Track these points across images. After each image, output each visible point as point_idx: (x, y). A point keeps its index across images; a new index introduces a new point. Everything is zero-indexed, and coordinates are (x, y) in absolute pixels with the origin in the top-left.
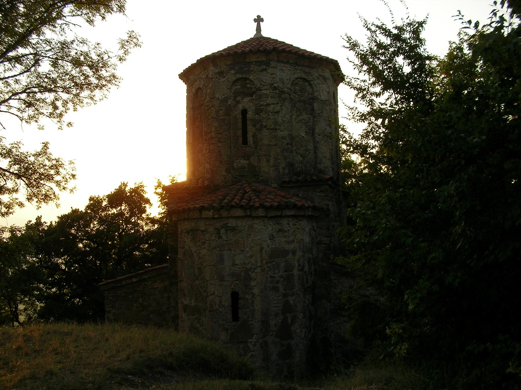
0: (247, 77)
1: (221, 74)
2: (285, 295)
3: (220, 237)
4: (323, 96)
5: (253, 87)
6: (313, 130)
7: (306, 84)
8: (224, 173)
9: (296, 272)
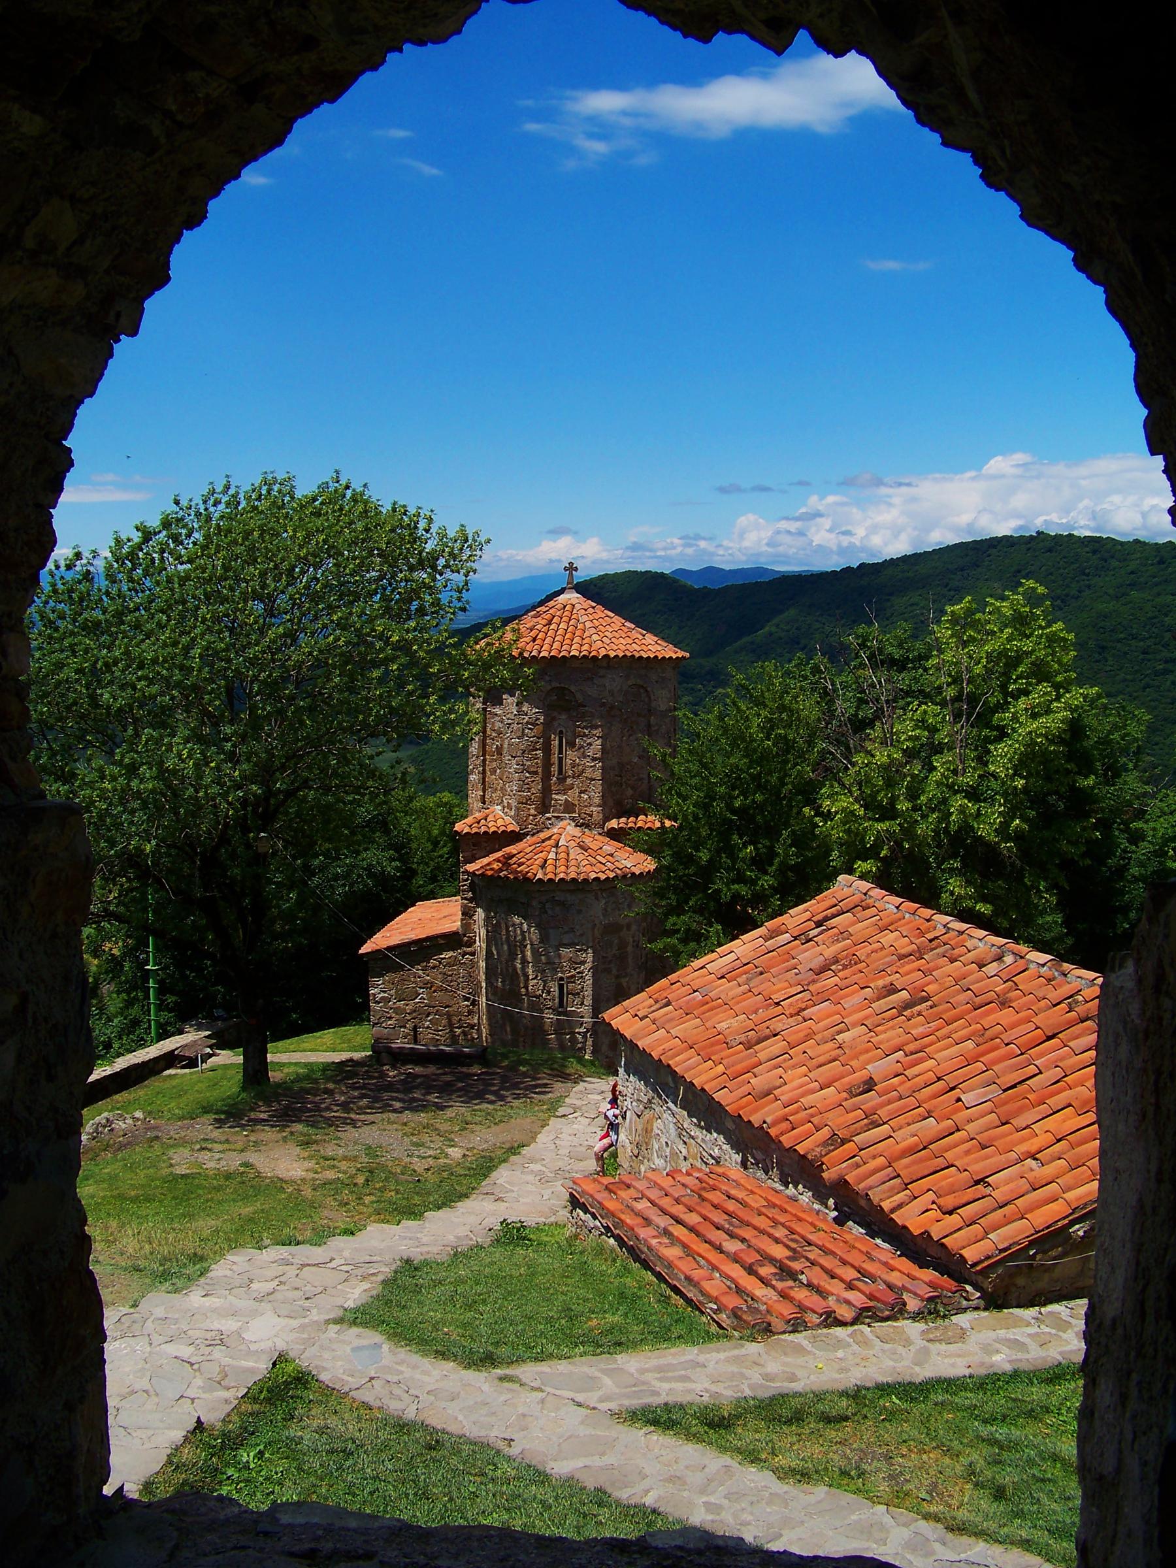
2: (617, 977)
3: (546, 912)
9: (630, 949)
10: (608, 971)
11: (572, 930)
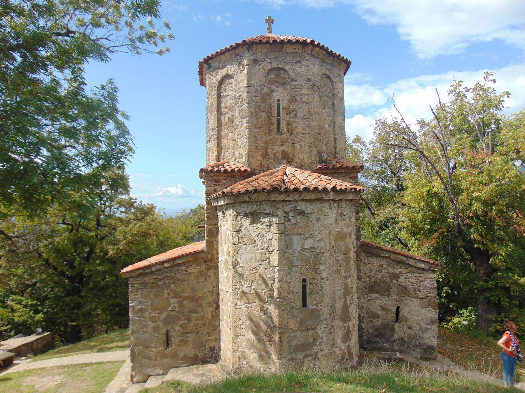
0: (282, 67)
1: (255, 62)
3: (289, 220)
4: (340, 95)
5: (287, 77)
6: (334, 123)
7: (328, 81)
8: (260, 158)
10: (339, 272)
11: (312, 236)
